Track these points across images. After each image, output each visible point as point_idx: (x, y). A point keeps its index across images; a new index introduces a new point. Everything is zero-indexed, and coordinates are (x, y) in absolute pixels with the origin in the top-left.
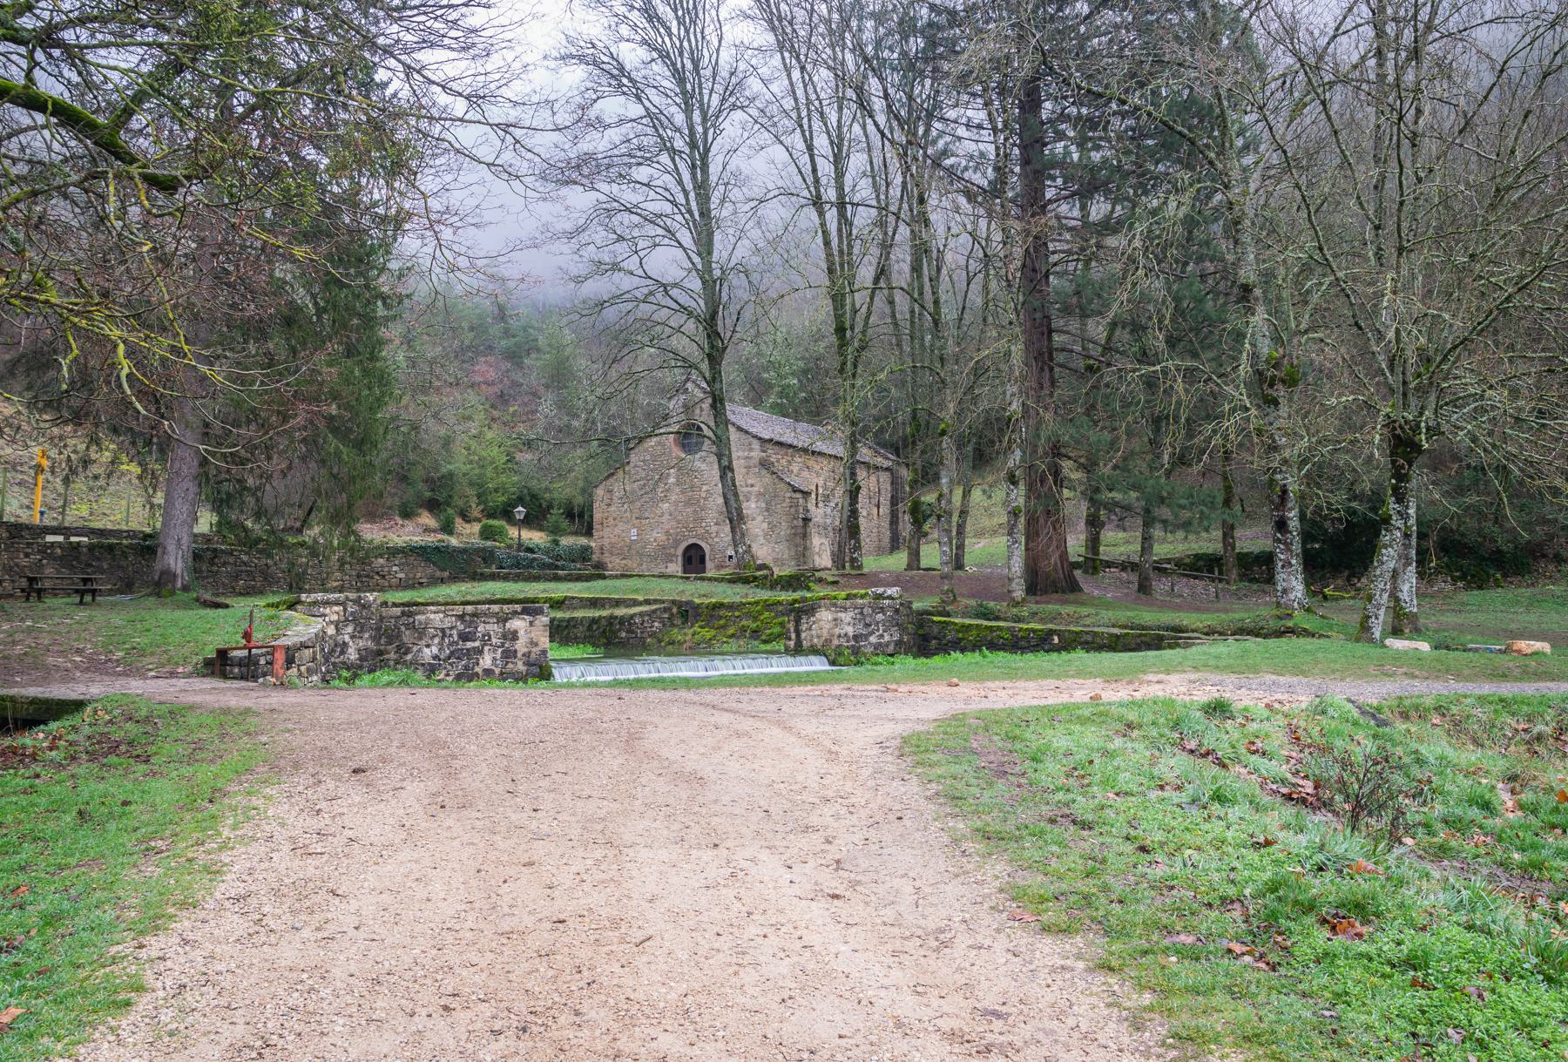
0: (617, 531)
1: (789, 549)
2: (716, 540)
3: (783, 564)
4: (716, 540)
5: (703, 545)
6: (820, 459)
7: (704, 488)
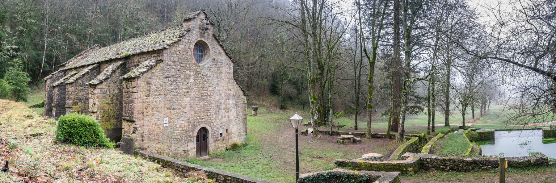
0: (154, 120)
4: (215, 124)
5: (208, 127)
7: (210, 89)
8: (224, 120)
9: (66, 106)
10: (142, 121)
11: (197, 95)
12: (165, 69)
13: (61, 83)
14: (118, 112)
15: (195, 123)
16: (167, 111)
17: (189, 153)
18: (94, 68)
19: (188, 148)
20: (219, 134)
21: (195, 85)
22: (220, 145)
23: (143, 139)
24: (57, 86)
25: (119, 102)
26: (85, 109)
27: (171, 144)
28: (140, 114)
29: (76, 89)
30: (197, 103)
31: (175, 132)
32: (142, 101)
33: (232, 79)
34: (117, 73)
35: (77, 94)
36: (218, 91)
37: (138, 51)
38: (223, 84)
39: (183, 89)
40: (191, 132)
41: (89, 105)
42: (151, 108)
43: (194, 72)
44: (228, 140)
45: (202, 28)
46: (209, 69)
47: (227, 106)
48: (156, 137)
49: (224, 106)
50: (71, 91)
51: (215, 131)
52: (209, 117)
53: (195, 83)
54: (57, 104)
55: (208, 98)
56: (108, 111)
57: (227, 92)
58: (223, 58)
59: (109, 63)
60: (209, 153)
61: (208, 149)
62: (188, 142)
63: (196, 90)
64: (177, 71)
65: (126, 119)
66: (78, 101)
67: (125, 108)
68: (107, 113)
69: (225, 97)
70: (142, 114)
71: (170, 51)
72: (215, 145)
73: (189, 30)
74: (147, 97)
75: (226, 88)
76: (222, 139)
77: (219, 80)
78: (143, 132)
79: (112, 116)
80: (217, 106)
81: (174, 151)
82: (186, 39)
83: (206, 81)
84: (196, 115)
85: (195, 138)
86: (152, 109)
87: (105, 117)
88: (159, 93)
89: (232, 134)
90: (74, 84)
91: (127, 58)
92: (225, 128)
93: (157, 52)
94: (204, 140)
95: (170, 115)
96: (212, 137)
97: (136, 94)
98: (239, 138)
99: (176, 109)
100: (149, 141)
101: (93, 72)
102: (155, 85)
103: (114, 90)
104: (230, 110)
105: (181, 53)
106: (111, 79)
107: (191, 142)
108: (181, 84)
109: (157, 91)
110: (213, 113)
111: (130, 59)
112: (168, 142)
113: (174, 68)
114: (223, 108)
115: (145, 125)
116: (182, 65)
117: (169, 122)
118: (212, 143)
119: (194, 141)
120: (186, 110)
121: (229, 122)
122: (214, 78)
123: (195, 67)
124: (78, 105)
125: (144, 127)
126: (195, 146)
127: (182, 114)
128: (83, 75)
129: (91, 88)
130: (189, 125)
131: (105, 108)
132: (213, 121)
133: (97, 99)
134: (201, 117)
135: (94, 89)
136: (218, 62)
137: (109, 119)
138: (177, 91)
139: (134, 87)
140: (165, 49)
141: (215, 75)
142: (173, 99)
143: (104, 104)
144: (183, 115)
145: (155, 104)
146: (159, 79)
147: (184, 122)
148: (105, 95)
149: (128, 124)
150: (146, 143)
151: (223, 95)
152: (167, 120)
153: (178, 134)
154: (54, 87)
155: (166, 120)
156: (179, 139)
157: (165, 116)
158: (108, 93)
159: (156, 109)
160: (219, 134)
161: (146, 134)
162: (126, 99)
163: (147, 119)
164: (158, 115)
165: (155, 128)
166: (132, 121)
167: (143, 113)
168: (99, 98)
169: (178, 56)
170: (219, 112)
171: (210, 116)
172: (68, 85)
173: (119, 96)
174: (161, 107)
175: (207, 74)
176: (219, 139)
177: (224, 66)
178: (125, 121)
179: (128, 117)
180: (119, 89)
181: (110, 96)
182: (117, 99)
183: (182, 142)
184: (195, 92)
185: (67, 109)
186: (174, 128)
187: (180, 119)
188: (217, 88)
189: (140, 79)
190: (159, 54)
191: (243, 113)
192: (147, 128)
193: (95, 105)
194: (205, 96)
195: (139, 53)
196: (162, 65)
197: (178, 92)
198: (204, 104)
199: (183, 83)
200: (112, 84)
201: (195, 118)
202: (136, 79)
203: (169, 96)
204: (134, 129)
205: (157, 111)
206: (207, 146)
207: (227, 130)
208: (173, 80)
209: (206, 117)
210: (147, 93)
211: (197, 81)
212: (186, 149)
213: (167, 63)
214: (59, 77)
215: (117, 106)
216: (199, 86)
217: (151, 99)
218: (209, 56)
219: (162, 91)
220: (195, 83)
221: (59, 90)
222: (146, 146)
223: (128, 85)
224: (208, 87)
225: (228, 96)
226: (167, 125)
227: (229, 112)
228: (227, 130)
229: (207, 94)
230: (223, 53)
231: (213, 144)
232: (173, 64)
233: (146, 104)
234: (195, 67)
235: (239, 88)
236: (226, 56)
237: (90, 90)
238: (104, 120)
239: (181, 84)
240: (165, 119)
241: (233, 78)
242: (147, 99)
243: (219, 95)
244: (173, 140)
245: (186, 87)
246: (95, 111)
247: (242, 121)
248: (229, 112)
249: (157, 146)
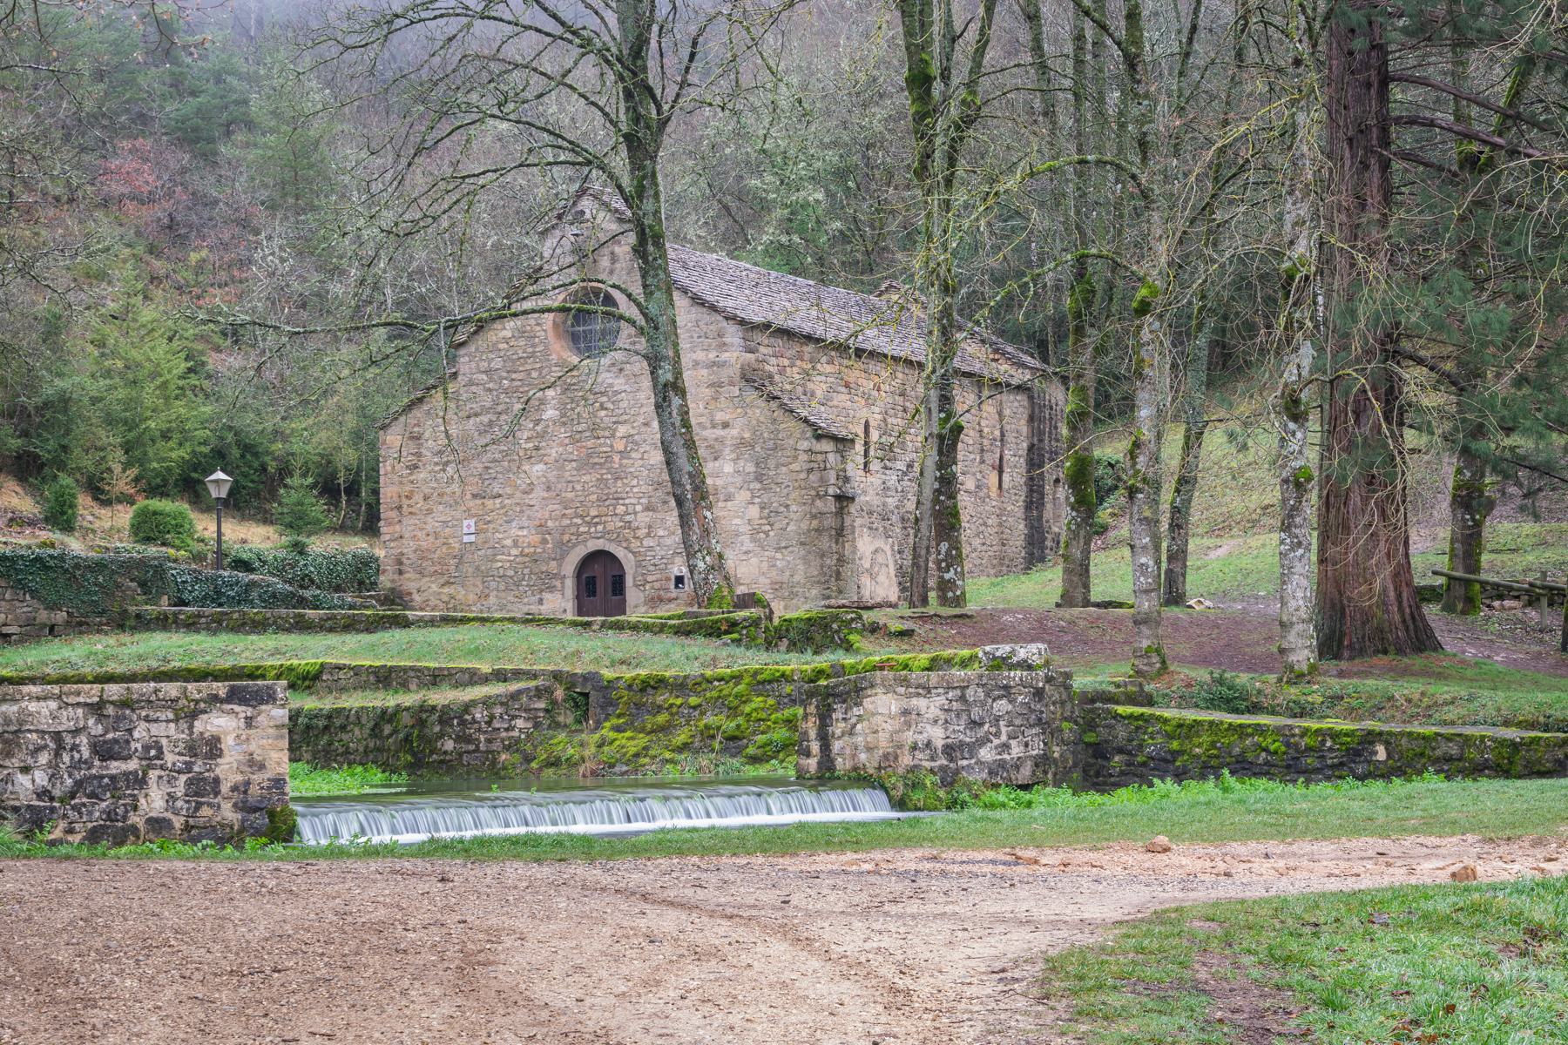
1: (806, 562)
2: (648, 542)
3: (793, 595)
4: (648, 542)
5: (620, 553)
6: (873, 366)
7: (622, 430)
10: (397, 528)
16: (471, 504)
20: (668, 579)
28: (392, 509)
31: (499, 557)
40: (554, 564)
48: (438, 568)
51: (652, 568)
52: (621, 521)
62: (542, 591)
63: (567, 441)
86: (426, 498)
99: (500, 496)
110: (638, 508)
112: (479, 583)
113: (490, 390)
116: (514, 376)
118: (636, 607)
125: (404, 541)
127: (518, 509)
130: (545, 541)
132: (642, 532)
145: (435, 485)
147: (525, 532)
150: (409, 579)
152: (472, 524)
155: (469, 527)
163: (412, 522)
167: (399, 508)
169: (502, 354)
171: (628, 518)
175: (611, 385)
176: (674, 595)
184: (561, 444)
187: (514, 524)
191: (807, 508)
217: (421, 475)
226: (472, 538)
229: (612, 446)
233: (408, 488)
240: (465, 523)
242: (411, 474)
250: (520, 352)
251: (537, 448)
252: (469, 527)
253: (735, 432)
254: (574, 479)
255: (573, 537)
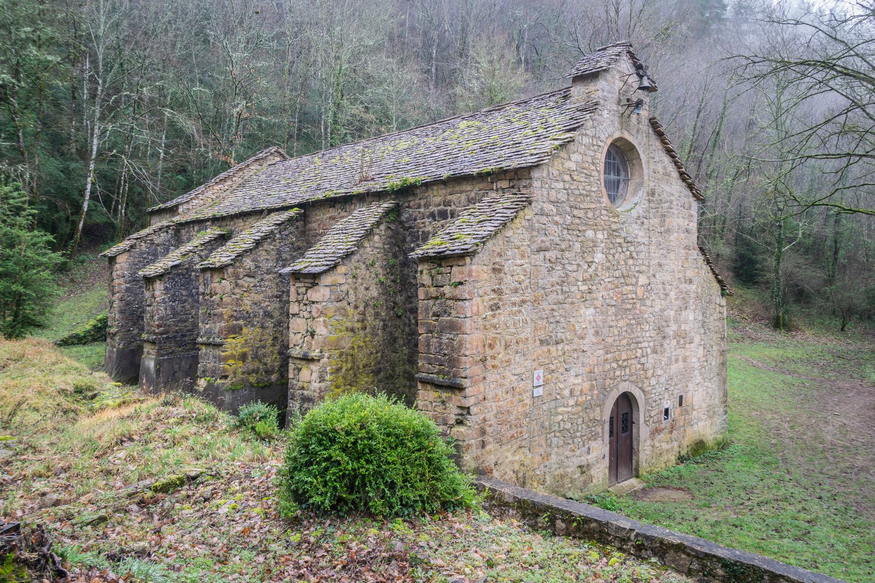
7: (643, 280)
8: (674, 368)
9: (200, 340)
11: (612, 298)
12: (537, 225)
13: (172, 267)
14: (379, 355)
15: (608, 381)
17: (593, 472)
18: (290, 220)
19: (589, 457)
21: (608, 268)
22: (665, 446)
23: (483, 441)
24: (160, 277)
25: (382, 323)
26: (264, 347)
27: (549, 449)
28: (477, 362)
29: (237, 285)
30: (612, 323)
31: (560, 410)
32: (481, 322)
33: (694, 249)
34: (376, 238)
35: (238, 302)
36: (660, 286)
37: (445, 173)
38: (673, 263)
39: (580, 283)
41: (291, 335)
42: (503, 344)
43: (605, 232)
44: (682, 429)
45: (625, 102)
46: (641, 220)
47: (683, 328)
48: (513, 432)
49: (674, 327)
50: (219, 290)
51: (654, 404)
53: (608, 264)
54: (161, 334)
55: (638, 305)
56: (351, 352)
57: (683, 286)
58: (675, 188)
59: (338, 206)
60: (637, 470)
61: (634, 457)
62: (590, 439)
63: (609, 286)
64: (565, 232)
65: (432, 379)
66: (241, 322)
67: (428, 345)
68: (350, 358)
69: (677, 303)
70: (481, 365)
71: (549, 172)
72: (653, 446)
73: (592, 107)
74: (492, 310)
75: (681, 275)
76: (668, 425)
77: (664, 252)
78: (485, 420)
79: (364, 367)
80: (659, 329)
81: (556, 469)
82: (586, 135)
83: (633, 258)
84: (609, 356)
85: (607, 427)
86: (507, 346)
87: (343, 370)
88: (521, 298)
89: (693, 409)
90: (230, 270)
91: (406, 191)
92: (676, 392)
93: (508, 176)
94: (625, 432)
95: (547, 361)
96: (645, 421)
97: (467, 303)
98: (708, 423)
100: (497, 445)
101: (287, 232)
102: (512, 276)
103: (367, 289)
104: (688, 339)
105: (575, 178)
106: (361, 255)
107: (595, 439)
108: (575, 267)
109: (516, 291)
110: (649, 350)
111: (414, 195)
112: (543, 442)
113: (556, 223)
114: (671, 333)
115: (490, 396)
116: (576, 212)
117: (546, 382)
118: (645, 441)
119: (603, 436)
120: (586, 344)
121: (686, 375)
122: (653, 248)
123: (606, 218)
124: (240, 334)
125: (487, 404)
126: (606, 450)
127: (575, 355)
128: (258, 243)
129: (298, 285)
131: (343, 343)
132: (650, 373)
133: (321, 319)
134: (620, 363)
135: (308, 288)
136: (661, 200)
137: (355, 375)
138: (565, 289)
139: (461, 283)
140: (537, 166)
141: (654, 239)
142: (555, 314)
143: (341, 331)
144: (578, 358)
145: (513, 330)
146: (523, 256)
148: (345, 303)
149: (436, 395)
151: (672, 295)
152: (541, 375)
153: (566, 416)
154: (149, 281)
155: (538, 378)
156: (568, 430)
157: (535, 364)
158: (352, 298)
159: (514, 347)
160: (661, 411)
161: (491, 426)
162: (431, 320)
164: (521, 364)
165: (512, 402)
166: (456, 388)
167: (484, 360)
168: (326, 315)
169: (567, 186)
170: (662, 345)
171: (643, 360)
172: (208, 275)
173: (382, 305)
174: (527, 339)
176: (663, 426)
177: (676, 212)
178: (429, 387)
179: (437, 373)
180: (382, 283)
181: (356, 307)
182: (377, 314)
183: (576, 440)
184: (606, 289)
185: (204, 349)
186: (556, 399)
187: (572, 372)
188: (657, 275)
189: (476, 260)
190: (515, 182)
192: (494, 405)
193: (313, 335)
194: (632, 301)
195: (449, 178)
196: (529, 213)
197: (566, 292)
198: (627, 324)
199: (578, 265)
200: (362, 271)
201: (608, 367)
202: (468, 259)
203: (544, 305)
204: (460, 411)
205: (517, 353)
206: (632, 448)
207: (681, 397)
208: (554, 257)
209: (633, 361)
210: (493, 299)
211: (611, 258)
212: (583, 460)
213: (542, 209)
214: (158, 245)
215: (377, 334)
216: (617, 273)
217: (503, 317)
218: (641, 184)
219: (529, 291)
220: (608, 264)
221: (166, 289)
222: (490, 460)
223: (439, 277)
224: (637, 275)
225: (683, 298)
227: (687, 346)
228: (681, 397)
229: (636, 293)
230: (675, 174)
231: (648, 442)
232: (555, 211)
233: (491, 334)
234: (606, 218)
235: (711, 276)
236: (680, 182)
237: (293, 290)
238: (340, 380)
239: (575, 267)
241: (696, 246)
242: (494, 316)
243: (662, 296)
244: (555, 436)
245: (587, 275)
246: (315, 354)
247: (716, 370)
248: (687, 346)
249: (517, 458)
250: (580, 188)
251: (590, 292)
252: (538, 378)
253: (693, 287)
254: (613, 324)
255: (612, 382)
